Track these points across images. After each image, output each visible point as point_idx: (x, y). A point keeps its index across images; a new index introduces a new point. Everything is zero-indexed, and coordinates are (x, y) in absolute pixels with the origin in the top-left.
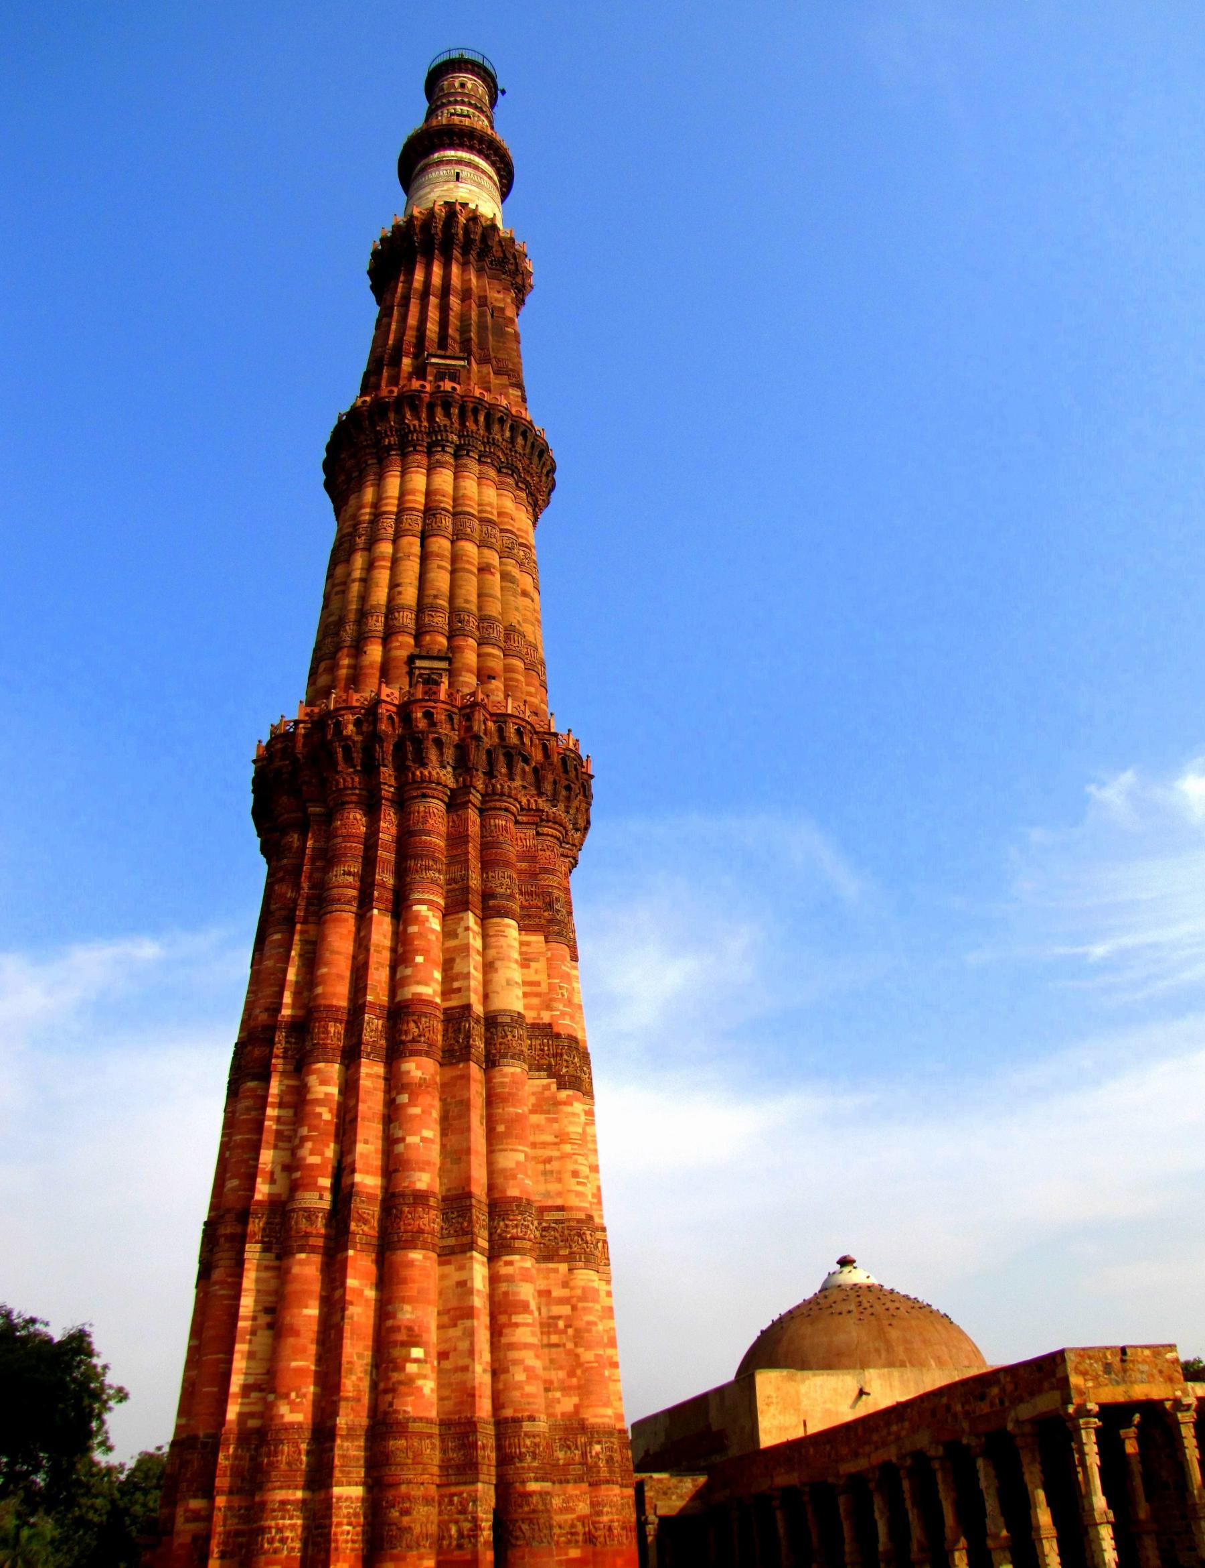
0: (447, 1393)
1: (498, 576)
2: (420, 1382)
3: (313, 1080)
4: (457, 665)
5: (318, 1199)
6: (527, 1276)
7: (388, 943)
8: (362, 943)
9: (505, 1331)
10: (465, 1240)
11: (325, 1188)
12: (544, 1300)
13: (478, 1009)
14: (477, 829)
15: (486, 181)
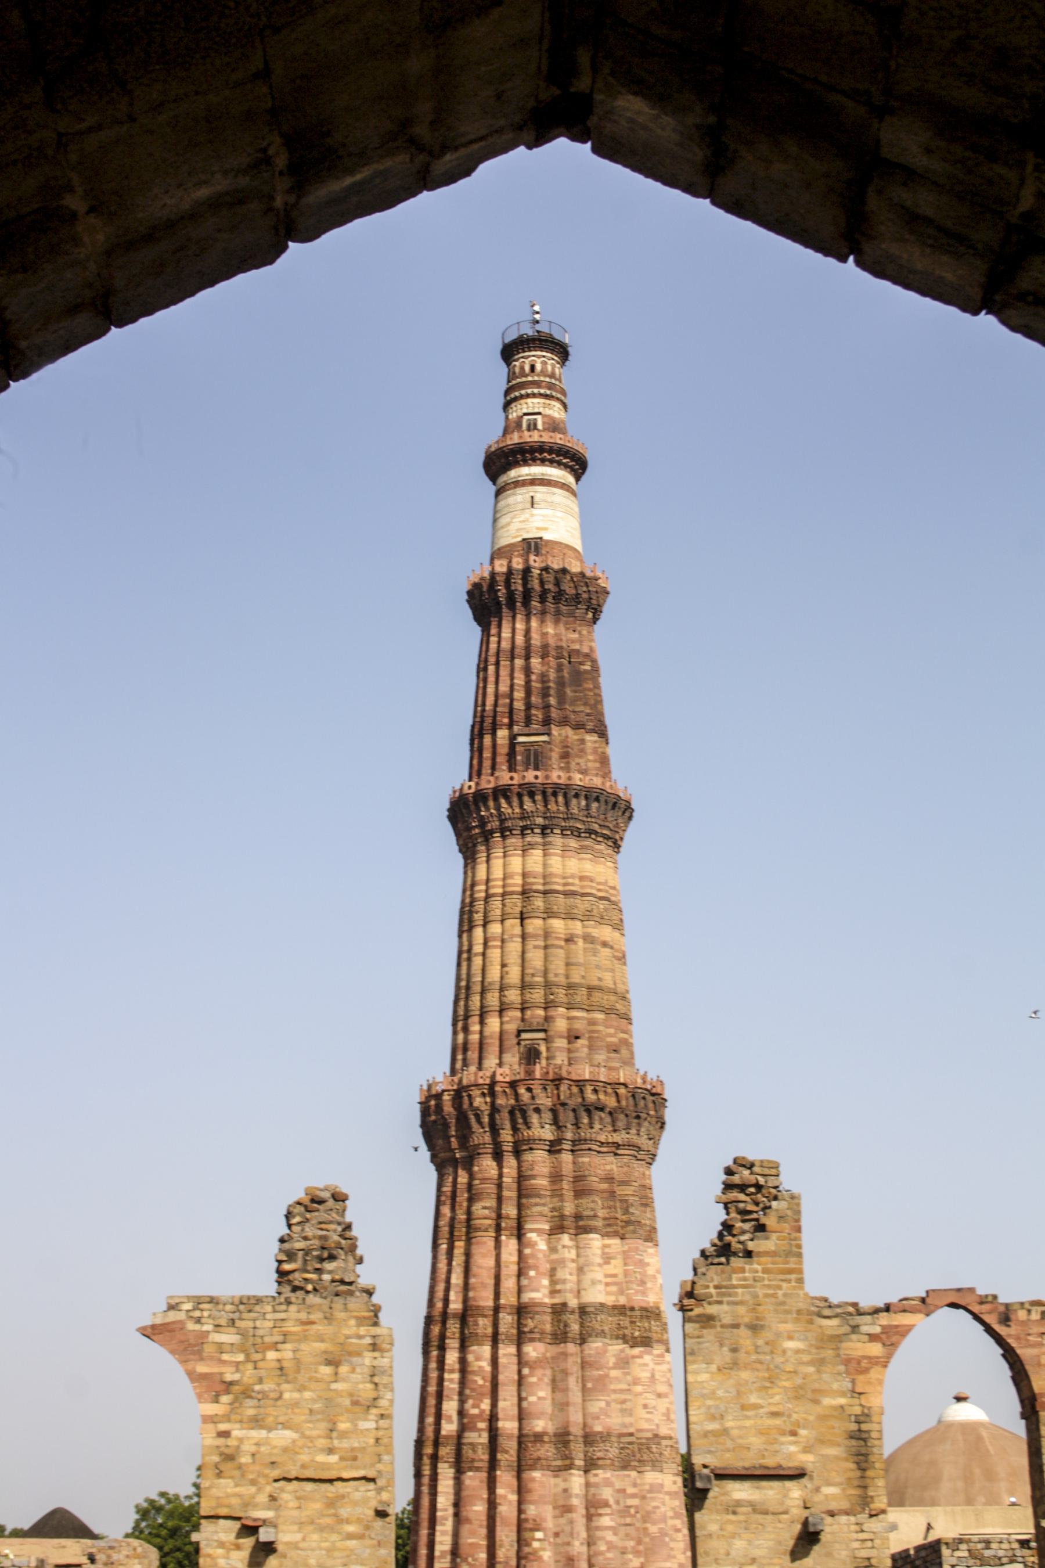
0: (559, 1558)
1: (580, 942)
2: (541, 1553)
3: (470, 1358)
4: (551, 1033)
5: (479, 1437)
6: (609, 1482)
7: (515, 1258)
8: (498, 1257)
9: (594, 1518)
10: (567, 1462)
11: (482, 1430)
12: (621, 1495)
13: (573, 1303)
14: (571, 1166)
15: (559, 496)
